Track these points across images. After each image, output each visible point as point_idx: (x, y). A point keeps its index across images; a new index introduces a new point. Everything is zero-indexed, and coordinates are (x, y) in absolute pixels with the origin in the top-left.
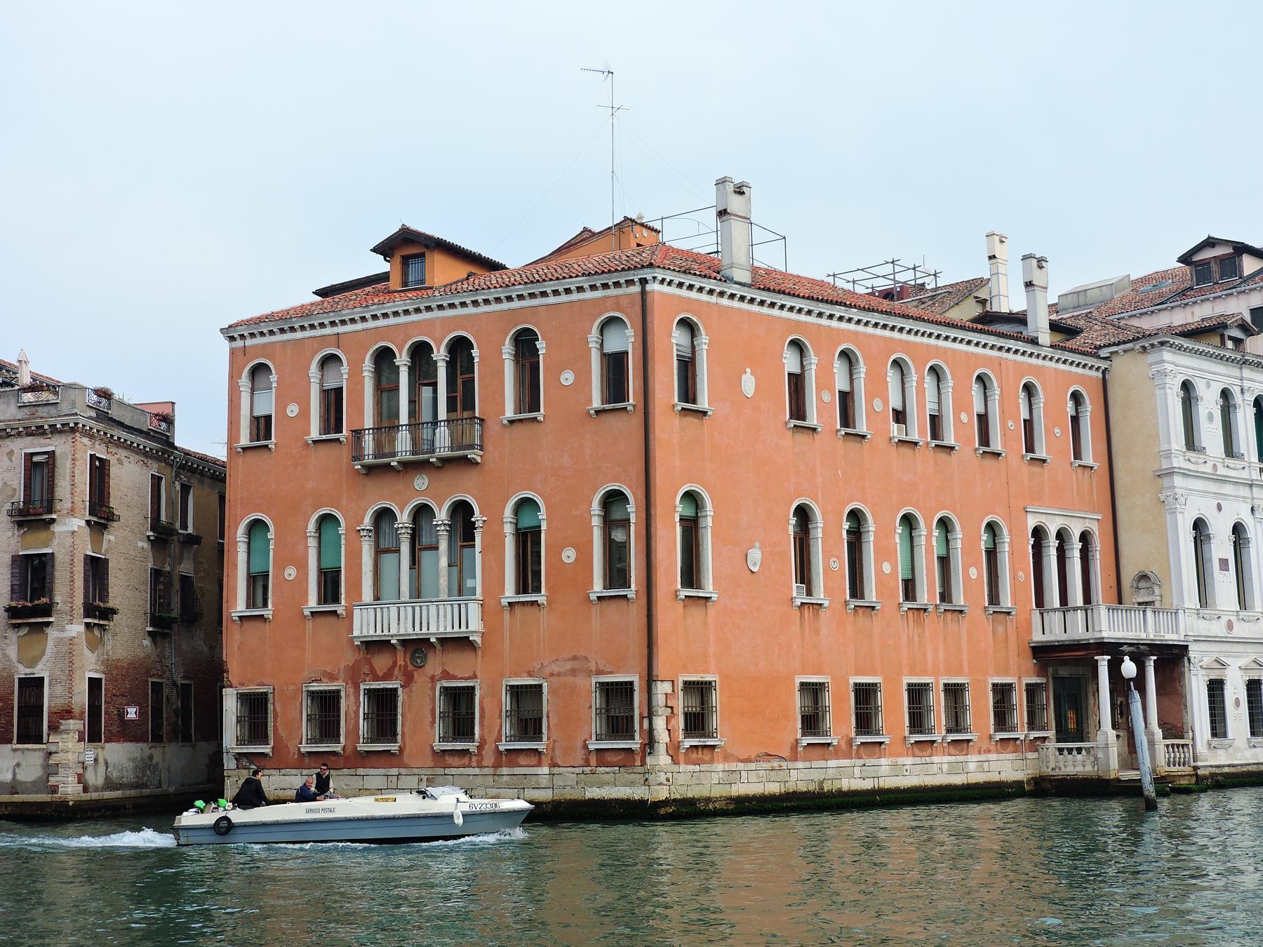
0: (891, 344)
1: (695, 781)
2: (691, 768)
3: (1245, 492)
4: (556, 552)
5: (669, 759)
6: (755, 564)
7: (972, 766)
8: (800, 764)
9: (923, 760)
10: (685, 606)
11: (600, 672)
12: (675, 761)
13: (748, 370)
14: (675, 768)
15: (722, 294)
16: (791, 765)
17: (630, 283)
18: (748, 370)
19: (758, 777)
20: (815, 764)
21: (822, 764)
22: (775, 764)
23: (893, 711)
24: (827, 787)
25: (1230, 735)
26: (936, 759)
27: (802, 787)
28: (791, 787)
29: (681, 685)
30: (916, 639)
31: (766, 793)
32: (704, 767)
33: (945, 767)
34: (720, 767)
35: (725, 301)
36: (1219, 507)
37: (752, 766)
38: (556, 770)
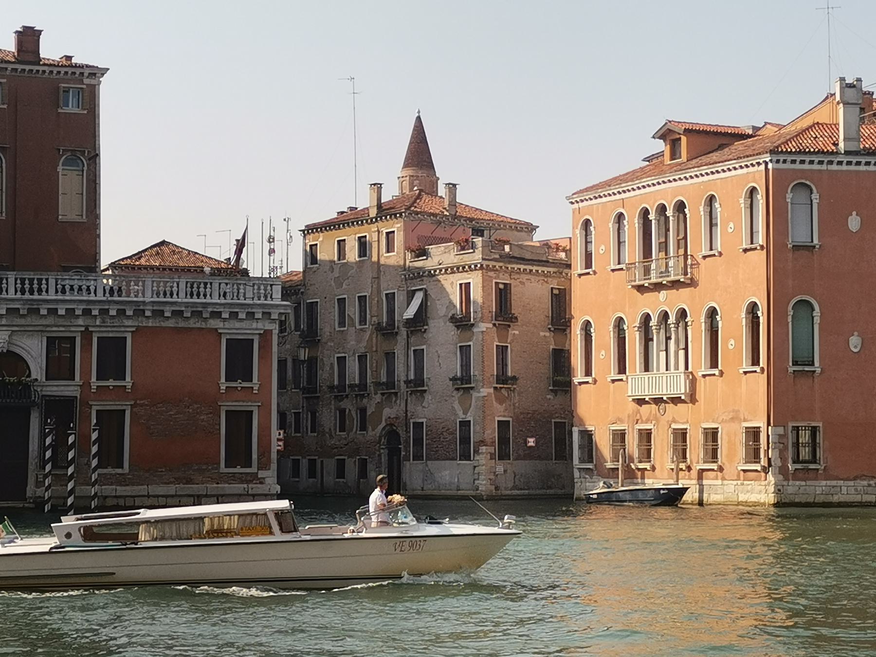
1: (801, 491)
2: (798, 483)
4: (726, 343)
5: (781, 477)
6: (856, 347)
10: (794, 377)
11: (745, 420)
12: (786, 479)
13: (854, 213)
14: (785, 483)
15: (831, 163)
17: (759, 164)
18: (854, 213)
19: (856, 490)
29: (790, 429)
31: (864, 501)
32: (809, 483)
34: (824, 483)
35: (834, 167)
37: (851, 483)
38: (725, 482)
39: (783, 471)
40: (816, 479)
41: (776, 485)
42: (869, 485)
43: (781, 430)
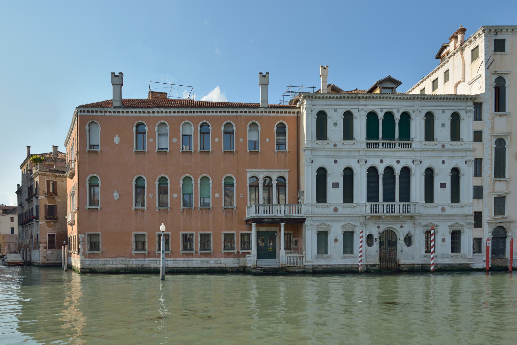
0: (183, 118)
3: (356, 154)
5: (83, 257)
6: (116, 197)
7: (212, 262)
8: (133, 259)
9: (188, 259)
10: (89, 212)
13: (117, 135)
16: (129, 259)
18: (117, 135)
20: (139, 259)
21: (143, 259)
22: (123, 259)
23: (217, 242)
24: (145, 266)
25: (329, 253)
26: (194, 259)
27: (134, 266)
28: (130, 266)
30: (187, 218)
32: (95, 259)
33: (199, 262)
34: (102, 259)
36: (336, 162)
37: (114, 259)
39: (84, 254)
40: (99, 258)
41: (81, 260)
42: (122, 260)
43: (83, 236)
